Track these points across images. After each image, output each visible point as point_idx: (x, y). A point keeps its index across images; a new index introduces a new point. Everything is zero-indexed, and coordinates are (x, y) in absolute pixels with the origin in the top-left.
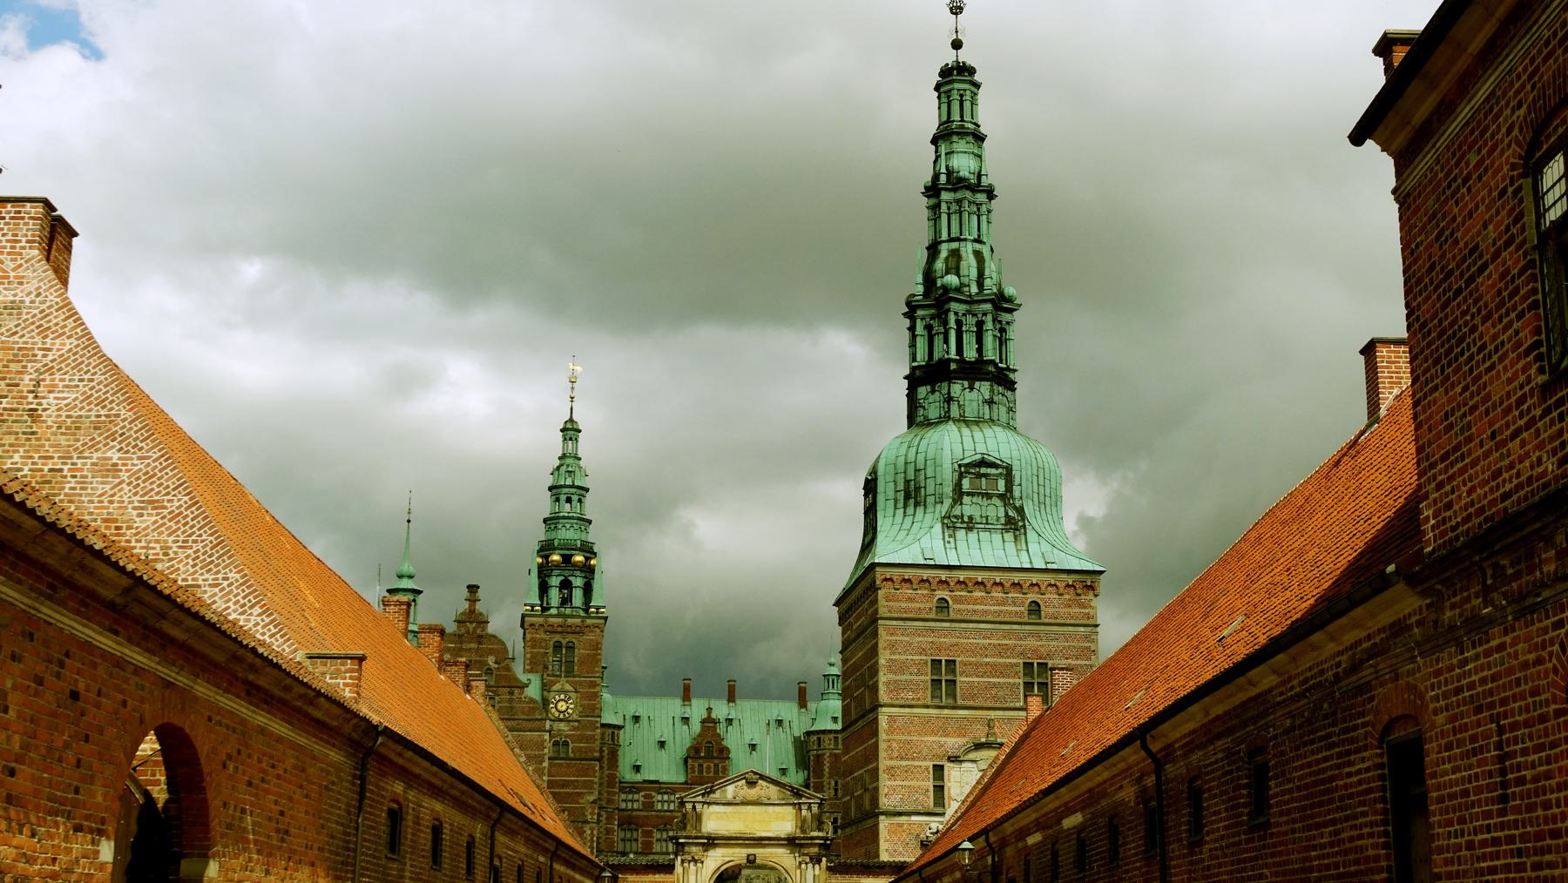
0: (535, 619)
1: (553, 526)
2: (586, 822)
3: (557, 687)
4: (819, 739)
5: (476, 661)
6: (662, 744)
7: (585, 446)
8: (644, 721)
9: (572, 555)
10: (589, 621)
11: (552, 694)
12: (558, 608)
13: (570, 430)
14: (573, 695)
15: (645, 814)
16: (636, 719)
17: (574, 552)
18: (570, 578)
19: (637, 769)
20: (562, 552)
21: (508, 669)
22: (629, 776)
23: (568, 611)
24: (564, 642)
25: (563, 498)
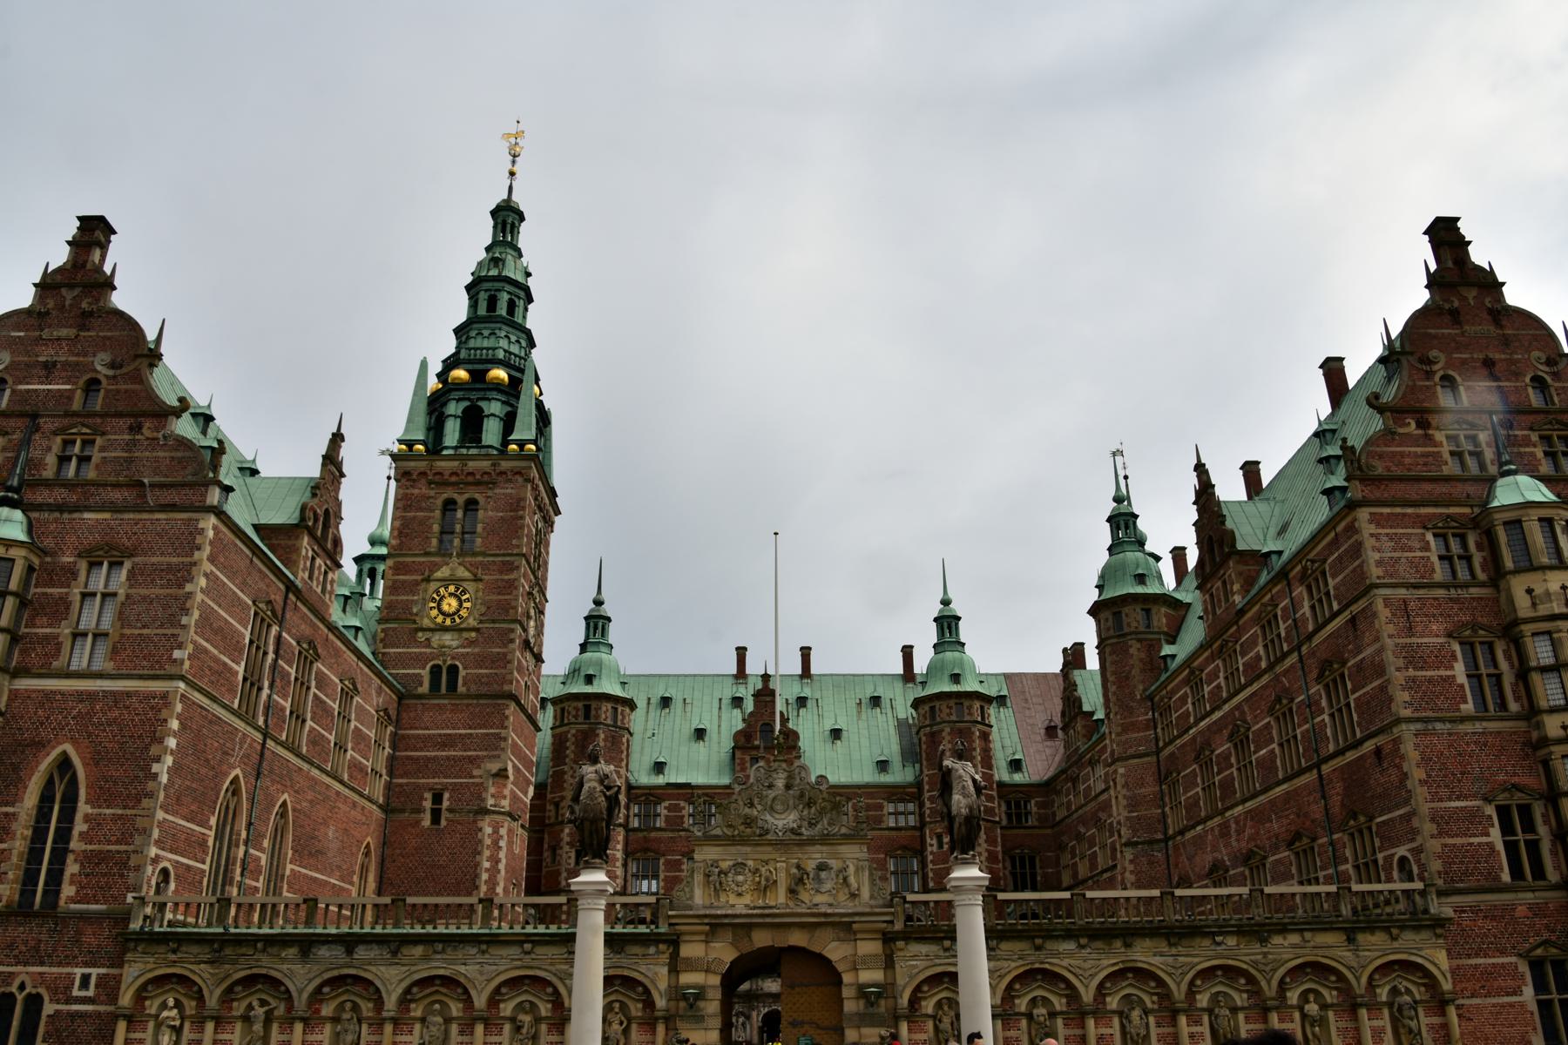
0: (412, 464)
1: (464, 339)
2: (487, 812)
3: (444, 572)
4: (932, 709)
5: (66, 364)
6: (700, 734)
7: (527, 237)
8: (677, 705)
9: (489, 370)
10: (505, 465)
11: (433, 586)
12: (456, 448)
13: (507, 217)
14: (470, 586)
15: (671, 835)
16: (666, 702)
17: (490, 366)
18: (480, 403)
19: (659, 767)
20: (470, 367)
21: (139, 379)
22: (644, 778)
23: (473, 451)
24: (461, 500)
25: (483, 296)
